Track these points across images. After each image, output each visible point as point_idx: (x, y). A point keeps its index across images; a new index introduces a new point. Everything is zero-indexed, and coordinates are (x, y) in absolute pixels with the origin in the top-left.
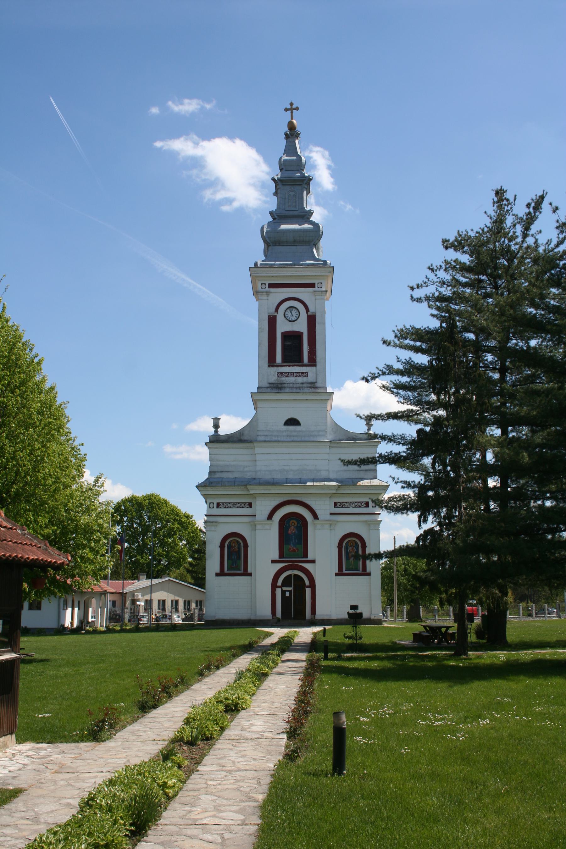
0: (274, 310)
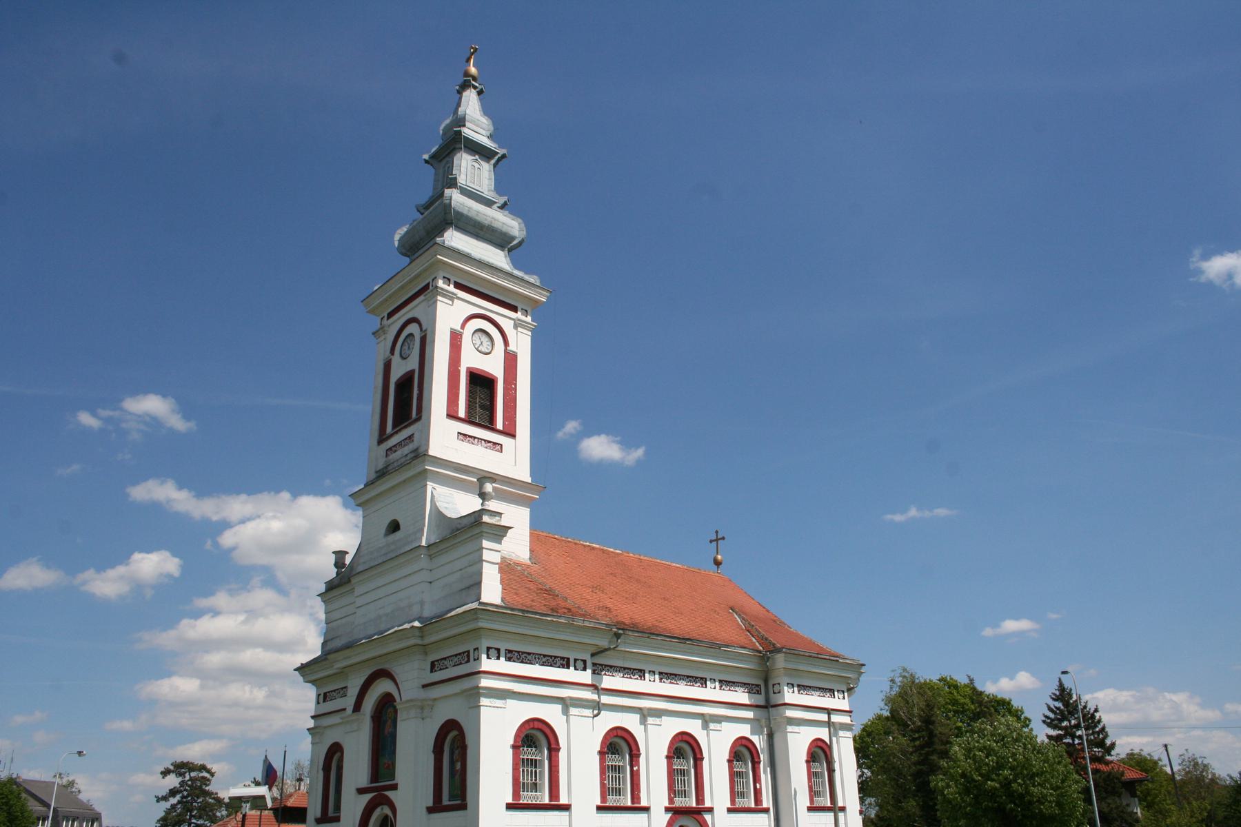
0: (388, 353)
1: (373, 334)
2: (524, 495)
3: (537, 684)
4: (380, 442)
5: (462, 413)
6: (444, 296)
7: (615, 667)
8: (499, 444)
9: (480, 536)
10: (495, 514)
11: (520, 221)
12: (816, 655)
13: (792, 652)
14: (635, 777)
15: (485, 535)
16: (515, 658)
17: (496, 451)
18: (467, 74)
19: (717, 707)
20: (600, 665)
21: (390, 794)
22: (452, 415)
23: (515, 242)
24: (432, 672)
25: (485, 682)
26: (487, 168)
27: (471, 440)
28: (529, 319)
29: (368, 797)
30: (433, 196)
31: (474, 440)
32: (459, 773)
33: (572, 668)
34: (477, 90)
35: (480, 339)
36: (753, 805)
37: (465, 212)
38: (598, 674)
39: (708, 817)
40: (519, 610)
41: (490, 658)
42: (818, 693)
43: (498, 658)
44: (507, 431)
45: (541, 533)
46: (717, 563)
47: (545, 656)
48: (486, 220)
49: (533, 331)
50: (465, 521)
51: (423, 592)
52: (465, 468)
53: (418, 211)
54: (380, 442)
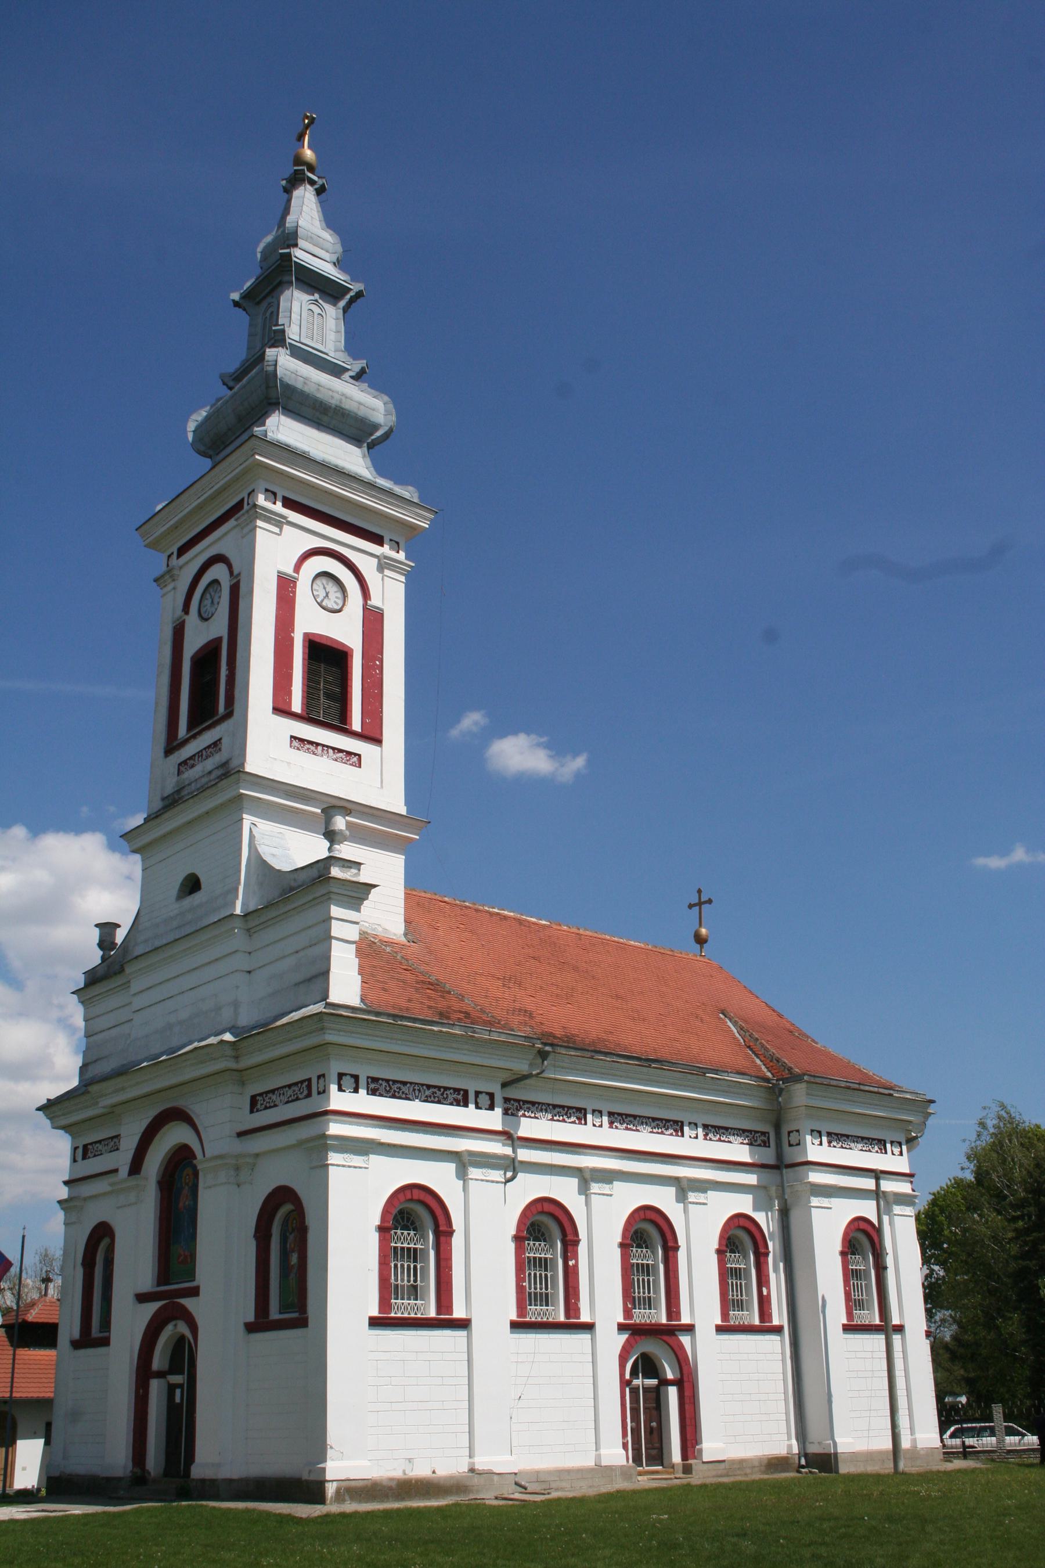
1: (155, 580)
2: (397, 835)
3: (417, 1131)
4: (169, 751)
5: (297, 706)
6: (268, 520)
7: (539, 1103)
8: (356, 754)
9: (327, 899)
10: (349, 865)
11: (386, 398)
12: (857, 1086)
13: (818, 1080)
14: (571, 1276)
15: (332, 896)
16: (382, 1090)
17: (350, 764)
18: (299, 160)
19: (700, 1167)
20: (515, 1100)
21: (187, 1302)
22: (281, 709)
23: (378, 434)
24: (252, 1112)
25: (336, 1128)
26: (332, 313)
27: (312, 748)
28: (401, 556)
29: (153, 1307)
30: (247, 360)
31: (316, 749)
32: (295, 1270)
33: (472, 1106)
34: (316, 186)
35: (325, 588)
36: (757, 1322)
37: (299, 385)
38: (513, 1115)
39: (685, 1340)
40: (389, 1015)
41: (344, 1091)
42: (860, 1146)
43: (356, 1091)
44: (366, 733)
45: (423, 894)
46: (700, 940)
47: (429, 1087)
48: (332, 397)
49: (408, 576)
50: (303, 876)
51: (237, 987)
52: (302, 791)
53: (224, 384)
54: (169, 751)
